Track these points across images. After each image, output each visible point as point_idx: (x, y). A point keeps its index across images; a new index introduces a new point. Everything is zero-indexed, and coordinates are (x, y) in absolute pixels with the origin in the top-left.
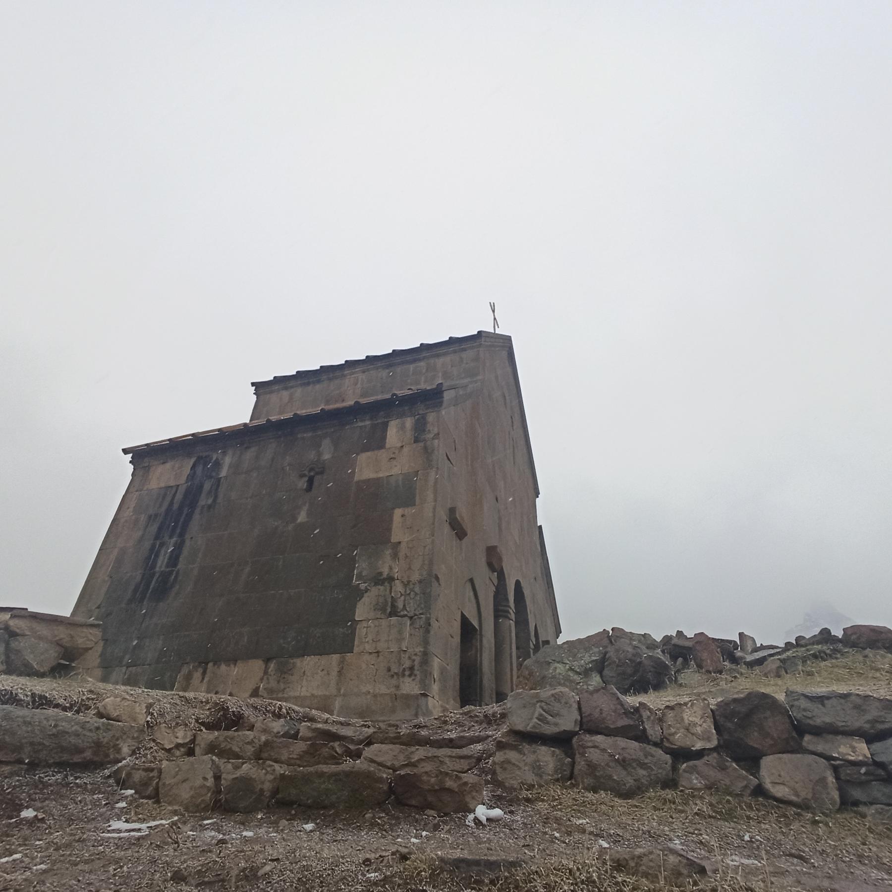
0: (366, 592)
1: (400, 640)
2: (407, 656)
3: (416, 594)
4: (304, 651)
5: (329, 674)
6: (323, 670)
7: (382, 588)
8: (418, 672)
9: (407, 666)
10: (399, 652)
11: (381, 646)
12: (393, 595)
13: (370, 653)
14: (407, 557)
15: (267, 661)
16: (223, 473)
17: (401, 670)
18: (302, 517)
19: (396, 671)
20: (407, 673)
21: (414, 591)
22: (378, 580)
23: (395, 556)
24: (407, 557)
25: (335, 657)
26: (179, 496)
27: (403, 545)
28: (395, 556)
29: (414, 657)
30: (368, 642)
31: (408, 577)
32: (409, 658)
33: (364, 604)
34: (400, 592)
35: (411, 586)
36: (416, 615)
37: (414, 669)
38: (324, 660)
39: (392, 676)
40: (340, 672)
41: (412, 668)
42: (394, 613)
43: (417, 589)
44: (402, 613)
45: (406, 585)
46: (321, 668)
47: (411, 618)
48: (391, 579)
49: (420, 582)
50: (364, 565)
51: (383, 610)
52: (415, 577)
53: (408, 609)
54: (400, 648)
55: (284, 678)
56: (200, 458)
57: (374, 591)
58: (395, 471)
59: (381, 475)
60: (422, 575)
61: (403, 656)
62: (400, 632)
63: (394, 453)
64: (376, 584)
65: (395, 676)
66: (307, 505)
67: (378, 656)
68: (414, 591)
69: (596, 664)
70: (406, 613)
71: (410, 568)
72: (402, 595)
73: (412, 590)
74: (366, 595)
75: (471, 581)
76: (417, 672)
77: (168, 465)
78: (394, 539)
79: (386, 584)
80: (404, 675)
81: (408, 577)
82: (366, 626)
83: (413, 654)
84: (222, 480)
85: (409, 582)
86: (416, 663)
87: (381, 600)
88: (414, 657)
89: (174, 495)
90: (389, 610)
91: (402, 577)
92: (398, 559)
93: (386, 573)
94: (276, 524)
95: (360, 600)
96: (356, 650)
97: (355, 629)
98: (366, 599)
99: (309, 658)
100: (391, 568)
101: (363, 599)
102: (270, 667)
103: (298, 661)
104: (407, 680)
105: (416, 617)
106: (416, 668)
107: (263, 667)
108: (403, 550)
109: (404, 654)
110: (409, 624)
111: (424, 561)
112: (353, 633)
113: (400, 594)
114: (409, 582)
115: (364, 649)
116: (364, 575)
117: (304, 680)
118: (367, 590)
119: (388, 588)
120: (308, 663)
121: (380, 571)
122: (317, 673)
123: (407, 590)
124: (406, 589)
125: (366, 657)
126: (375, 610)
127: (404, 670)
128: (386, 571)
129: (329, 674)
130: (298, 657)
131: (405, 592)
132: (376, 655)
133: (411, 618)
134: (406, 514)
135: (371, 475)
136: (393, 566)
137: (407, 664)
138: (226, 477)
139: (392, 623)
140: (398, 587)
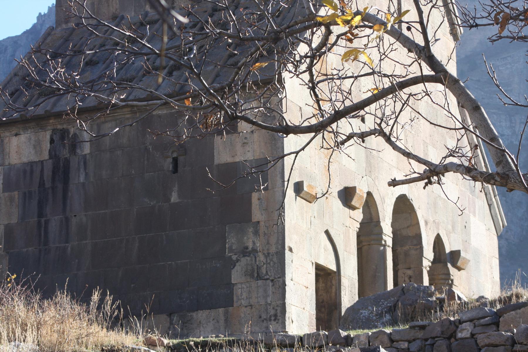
0: (237, 262)
1: (266, 297)
2: (272, 307)
3: (274, 263)
4: (199, 306)
5: (218, 322)
6: (214, 319)
7: (249, 258)
8: (280, 318)
9: (273, 314)
10: (266, 305)
11: (253, 301)
12: (257, 263)
13: (246, 307)
14: (265, 234)
15: (170, 315)
16: (87, 149)
17: (268, 317)
18: (174, 198)
19: (265, 317)
20: (273, 318)
21: (272, 261)
22: (245, 252)
23: (256, 233)
24: (265, 234)
25: (221, 310)
26: (48, 173)
27: (262, 224)
28: (256, 233)
29: (277, 308)
30: (243, 299)
31: (268, 250)
32: (273, 308)
33: (237, 271)
34: (263, 261)
35: (271, 257)
36: (275, 278)
37: (277, 316)
38: (213, 313)
39: (263, 321)
40: (226, 320)
41: (276, 315)
42: (259, 277)
43: (275, 259)
44: (266, 277)
45: (267, 256)
46: (212, 318)
47: (272, 281)
48: (254, 251)
49: (277, 253)
50: (233, 241)
51: (252, 276)
52: (273, 249)
53: (270, 274)
54: (266, 302)
55: (186, 326)
56: (54, 131)
57: (244, 261)
58: (250, 156)
59: (237, 160)
60: (278, 249)
61: (269, 307)
62: (265, 291)
63: (246, 138)
64: (244, 256)
65: (265, 321)
66: (176, 186)
67: (252, 308)
68: (272, 261)
69: (390, 308)
70: (268, 277)
71: (268, 243)
72: (264, 264)
73: (271, 260)
74: (237, 264)
75: (327, 232)
76: (278, 318)
77: (23, 137)
78: (255, 218)
79: (252, 255)
80: (270, 320)
81: (268, 250)
82: (240, 287)
83: (275, 306)
84: (88, 156)
85: (268, 254)
86: (278, 311)
87: (249, 268)
88: (277, 308)
89: (42, 171)
90: (256, 275)
91: (263, 250)
92: (259, 235)
93: (251, 247)
94: (152, 203)
95: (234, 267)
96: (235, 305)
97: (233, 290)
98: (238, 267)
99: (201, 312)
100: (254, 243)
101: (236, 268)
102: (173, 319)
103: (194, 314)
104: (273, 323)
105: (275, 280)
106: (279, 315)
107: (169, 319)
108: (262, 228)
109: (269, 306)
110: (271, 285)
111: (278, 238)
112: (232, 293)
113: (262, 263)
114: (268, 254)
115: (241, 304)
116: (234, 248)
117: (201, 327)
118: (238, 261)
119: (254, 259)
120: (201, 315)
121: (246, 245)
122: (210, 322)
123: (268, 259)
124: (267, 259)
125: (243, 309)
126: (245, 275)
127: (271, 317)
128: (250, 246)
129: (218, 322)
130: (193, 311)
131: (267, 261)
132: (250, 307)
133: (272, 281)
134: (262, 197)
135: (230, 160)
136: (256, 241)
137: (272, 312)
138: (90, 154)
139: (259, 285)
140: (261, 257)
